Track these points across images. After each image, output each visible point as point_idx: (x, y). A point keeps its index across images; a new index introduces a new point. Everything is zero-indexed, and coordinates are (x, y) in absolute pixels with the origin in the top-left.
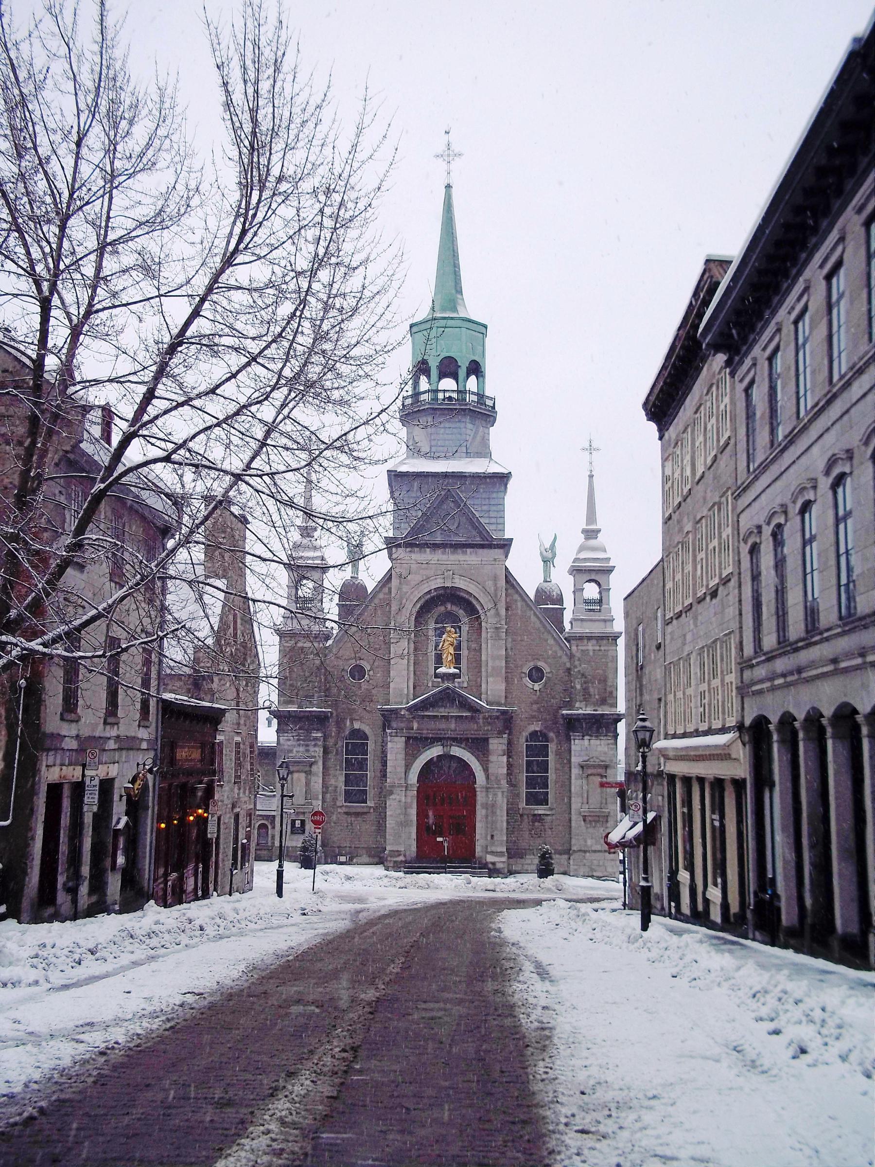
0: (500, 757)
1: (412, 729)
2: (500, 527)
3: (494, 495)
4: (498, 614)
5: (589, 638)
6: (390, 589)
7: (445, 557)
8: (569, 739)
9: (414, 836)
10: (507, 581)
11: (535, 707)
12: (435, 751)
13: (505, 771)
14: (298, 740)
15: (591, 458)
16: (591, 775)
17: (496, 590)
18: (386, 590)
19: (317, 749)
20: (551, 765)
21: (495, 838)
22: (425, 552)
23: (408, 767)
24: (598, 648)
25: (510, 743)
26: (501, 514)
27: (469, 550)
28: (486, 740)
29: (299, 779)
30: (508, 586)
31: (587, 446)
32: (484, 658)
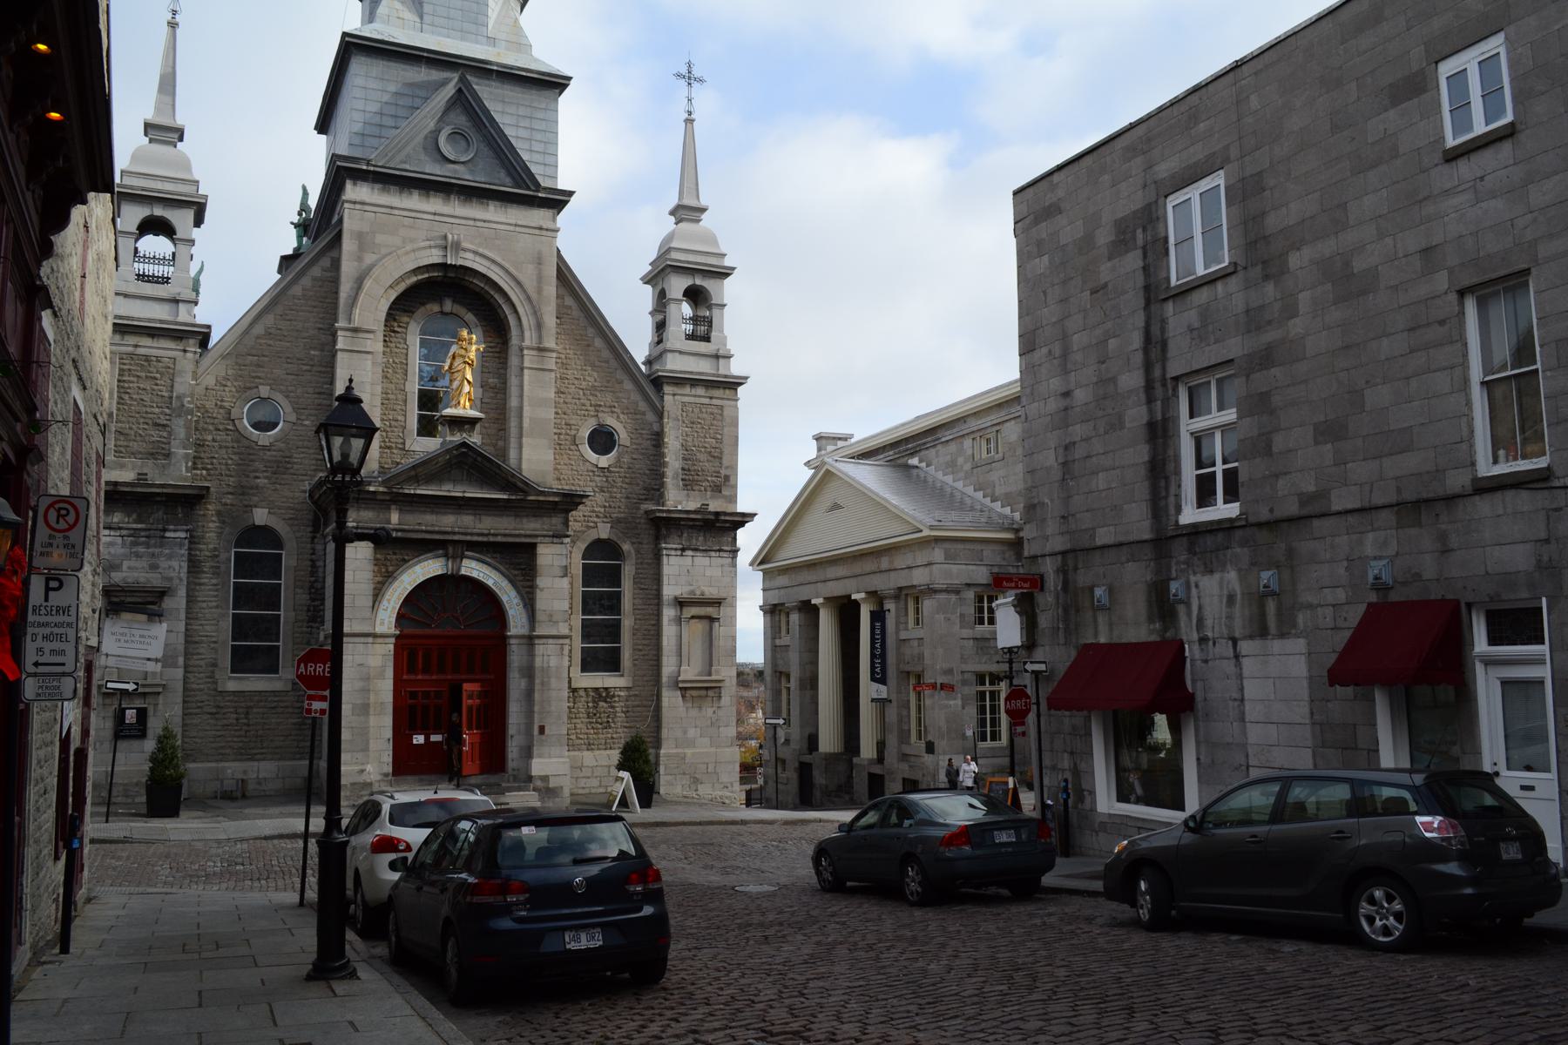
0: (557, 580)
1: (389, 522)
3: (540, 115)
4: (539, 326)
5: (694, 383)
7: (446, 209)
9: (389, 733)
10: (559, 270)
12: (428, 568)
14: (134, 544)
15: (690, 92)
16: (693, 617)
17: (540, 278)
18: (326, 262)
19: (175, 564)
20: (627, 603)
21: (547, 731)
22: (411, 193)
23: (377, 594)
24: (707, 401)
28: (533, 546)
31: (684, 71)
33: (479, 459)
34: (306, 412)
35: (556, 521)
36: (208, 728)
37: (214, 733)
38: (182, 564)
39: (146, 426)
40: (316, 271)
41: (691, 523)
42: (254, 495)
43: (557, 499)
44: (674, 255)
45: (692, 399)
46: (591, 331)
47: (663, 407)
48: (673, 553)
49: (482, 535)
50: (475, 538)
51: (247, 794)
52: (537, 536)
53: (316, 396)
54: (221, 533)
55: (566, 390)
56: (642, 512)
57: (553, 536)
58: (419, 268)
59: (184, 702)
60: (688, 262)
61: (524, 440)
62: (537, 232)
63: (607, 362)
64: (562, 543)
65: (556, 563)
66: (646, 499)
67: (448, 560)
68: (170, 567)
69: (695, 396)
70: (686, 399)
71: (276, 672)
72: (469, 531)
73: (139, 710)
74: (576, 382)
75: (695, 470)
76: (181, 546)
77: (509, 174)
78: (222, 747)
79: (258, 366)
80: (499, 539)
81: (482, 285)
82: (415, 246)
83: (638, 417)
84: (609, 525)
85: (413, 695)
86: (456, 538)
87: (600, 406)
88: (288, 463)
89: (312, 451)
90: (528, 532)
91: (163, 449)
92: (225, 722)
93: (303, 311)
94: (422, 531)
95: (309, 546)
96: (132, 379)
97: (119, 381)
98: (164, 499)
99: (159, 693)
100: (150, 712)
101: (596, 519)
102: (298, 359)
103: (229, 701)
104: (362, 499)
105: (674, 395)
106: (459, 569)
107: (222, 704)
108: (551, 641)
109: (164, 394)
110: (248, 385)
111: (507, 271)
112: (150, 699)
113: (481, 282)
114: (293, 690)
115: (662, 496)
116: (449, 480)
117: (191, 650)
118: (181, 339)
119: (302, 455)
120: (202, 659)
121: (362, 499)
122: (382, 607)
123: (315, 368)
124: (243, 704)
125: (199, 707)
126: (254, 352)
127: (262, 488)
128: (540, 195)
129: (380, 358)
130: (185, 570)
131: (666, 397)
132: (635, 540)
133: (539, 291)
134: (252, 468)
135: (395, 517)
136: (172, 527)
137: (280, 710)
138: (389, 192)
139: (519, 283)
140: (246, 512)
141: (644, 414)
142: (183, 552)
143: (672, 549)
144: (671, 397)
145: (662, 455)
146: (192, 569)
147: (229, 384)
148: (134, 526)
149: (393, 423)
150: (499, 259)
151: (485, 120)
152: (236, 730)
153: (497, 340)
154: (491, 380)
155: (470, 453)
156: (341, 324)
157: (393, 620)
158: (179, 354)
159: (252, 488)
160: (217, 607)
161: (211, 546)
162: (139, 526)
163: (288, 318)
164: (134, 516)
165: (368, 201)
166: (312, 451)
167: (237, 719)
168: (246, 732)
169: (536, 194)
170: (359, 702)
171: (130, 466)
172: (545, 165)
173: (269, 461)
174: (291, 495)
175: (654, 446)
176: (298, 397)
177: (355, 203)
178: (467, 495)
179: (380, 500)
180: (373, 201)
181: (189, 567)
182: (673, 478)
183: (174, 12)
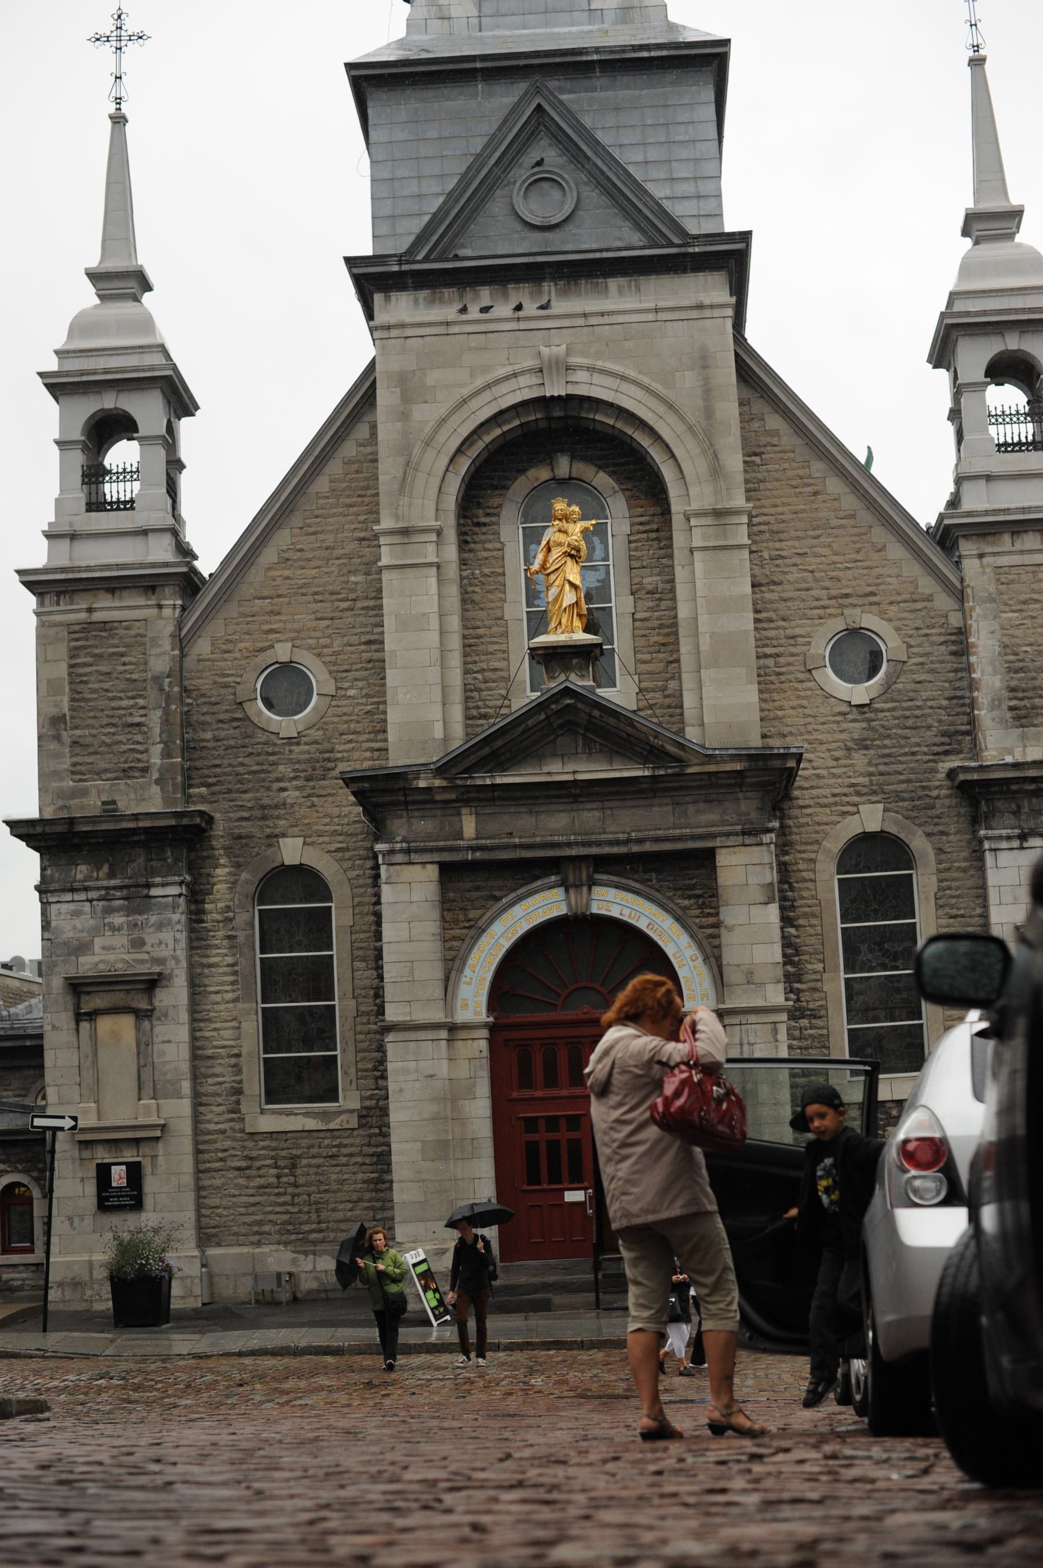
0: (756, 910)
1: (460, 836)
2: (707, 207)
4: (716, 471)
6: (374, 427)
8: (978, 857)
11: (860, 760)
13: (776, 953)
14: (108, 911)
17: (708, 392)
18: (362, 431)
19: (167, 936)
25: (784, 870)
26: (708, 168)
27: (613, 283)
28: (710, 854)
29: (115, 1035)
30: (748, 394)
32: (683, 612)
33: (596, 713)
34: (351, 675)
35: (748, 806)
36: (237, 1193)
37: (245, 1199)
38: (178, 935)
39: (112, 730)
40: (349, 449)
41: (1032, 787)
42: (278, 818)
43: (738, 767)
44: (960, 306)
45: (1017, 559)
46: (818, 467)
47: (962, 580)
48: (1004, 845)
49: (617, 843)
50: (607, 850)
51: (299, 1295)
52: (713, 836)
53: (363, 647)
54: (233, 883)
55: (781, 577)
56: (941, 776)
57: (744, 833)
58: (501, 413)
59: (198, 1152)
60: (985, 313)
61: (704, 673)
62: (694, 314)
63: (853, 516)
64: (761, 844)
65: (753, 880)
66: (947, 753)
67: (567, 891)
68: (161, 943)
69: (1022, 552)
70: (1005, 561)
71: (336, 1099)
72: (593, 838)
73: (128, 1164)
74: (797, 560)
75: (1034, 689)
76: (175, 907)
77: (638, 227)
78: (260, 1223)
79: (272, 613)
80: (648, 847)
81: (611, 422)
82: (490, 377)
83: (919, 605)
84: (881, 806)
85: (531, 1124)
86: (574, 852)
87: (847, 596)
88: (329, 760)
89: (366, 736)
90: (700, 831)
91: (139, 760)
92: (262, 1181)
93: (335, 515)
94: (515, 846)
95: (370, 890)
96: (89, 660)
97: (71, 666)
98: (143, 838)
99: (157, 1139)
100: (147, 1169)
101: (856, 799)
102: (332, 593)
103: (264, 1148)
104: (414, 802)
105: (981, 556)
106: (588, 906)
107: (254, 1154)
108: (753, 1018)
109: (135, 676)
110: (260, 645)
111: (647, 390)
112: (145, 1149)
113: (607, 415)
114: (361, 1126)
115: (975, 742)
116: (554, 755)
117: (203, 1070)
118: (153, 589)
119: (352, 745)
120: (220, 1083)
121: (414, 802)
122: (464, 979)
123: (359, 604)
124: (284, 1153)
125: (221, 1160)
126: (266, 593)
127: (292, 805)
128: (691, 250)
129: (452, 571)
130: (183, 944)
131: (966, 563)
132: (929, 829)
133: (709, 413)
134: (273, 776)
135: (469, 826)
136: (158, 880)
137: (344, 1160)
138: (442, 301)
139: (671, 406)
140: (270, 845)
141: (929, 599)
142: (176, 917)
143: (1000, 838)
144: (976, 562)
145: (969, 668)
146: (196, 944)
147: (229, 647)
148: (105, 883)
149: (489, 675)
150: (632, 373)
151: (584, 147)
152: (278, 1194)
153: (652, 510)
154: (645, 581)
155: (580, 705)
156: (387, 523)
157: (483, 999)
158: (154, 611)
159: (276, 807)
160: (235, 1000)
161: (221, 905)
162: (113, 882)
163: (312, 530)
164: (106, 868)
165: (408, 319)
166: (366, 736)
167: (278, 1177)
168: (293, 1196)
169: (683, 250)
170: (430, 1137)
171: (94, 792)
172: (699, 197)
173: (299, 762)
174: (336, 811)
175: (953, 653)
176: (336, 654)
177: (389, 328)
178: (580, 777)
179: (443, 802)
180: (418, 319)
181: (190, 940)
182: (992, 708)
183: (118, 100)
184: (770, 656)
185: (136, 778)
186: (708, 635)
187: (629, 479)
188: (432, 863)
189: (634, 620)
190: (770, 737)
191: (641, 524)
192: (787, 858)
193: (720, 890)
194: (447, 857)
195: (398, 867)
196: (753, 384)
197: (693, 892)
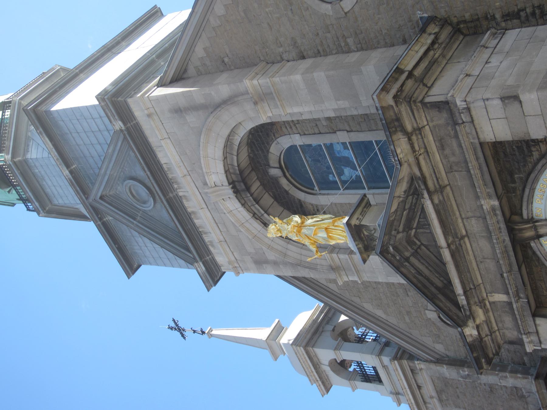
62: (156, 117)
64: (468, 109)
67: (541, 236)
169: (126, 132)
184: (346, 42)
185: (523, 393)
186: (338, 102)
187: (268, 134)
188: (534, 321)
189: (352, 131)
190: (404, 36)
191: (291, 128)
192: (498, 16)
193: (516, 139)
194: (528, 313)
195: (542, 339)
196: (185, 64)
197: (525, 149)
